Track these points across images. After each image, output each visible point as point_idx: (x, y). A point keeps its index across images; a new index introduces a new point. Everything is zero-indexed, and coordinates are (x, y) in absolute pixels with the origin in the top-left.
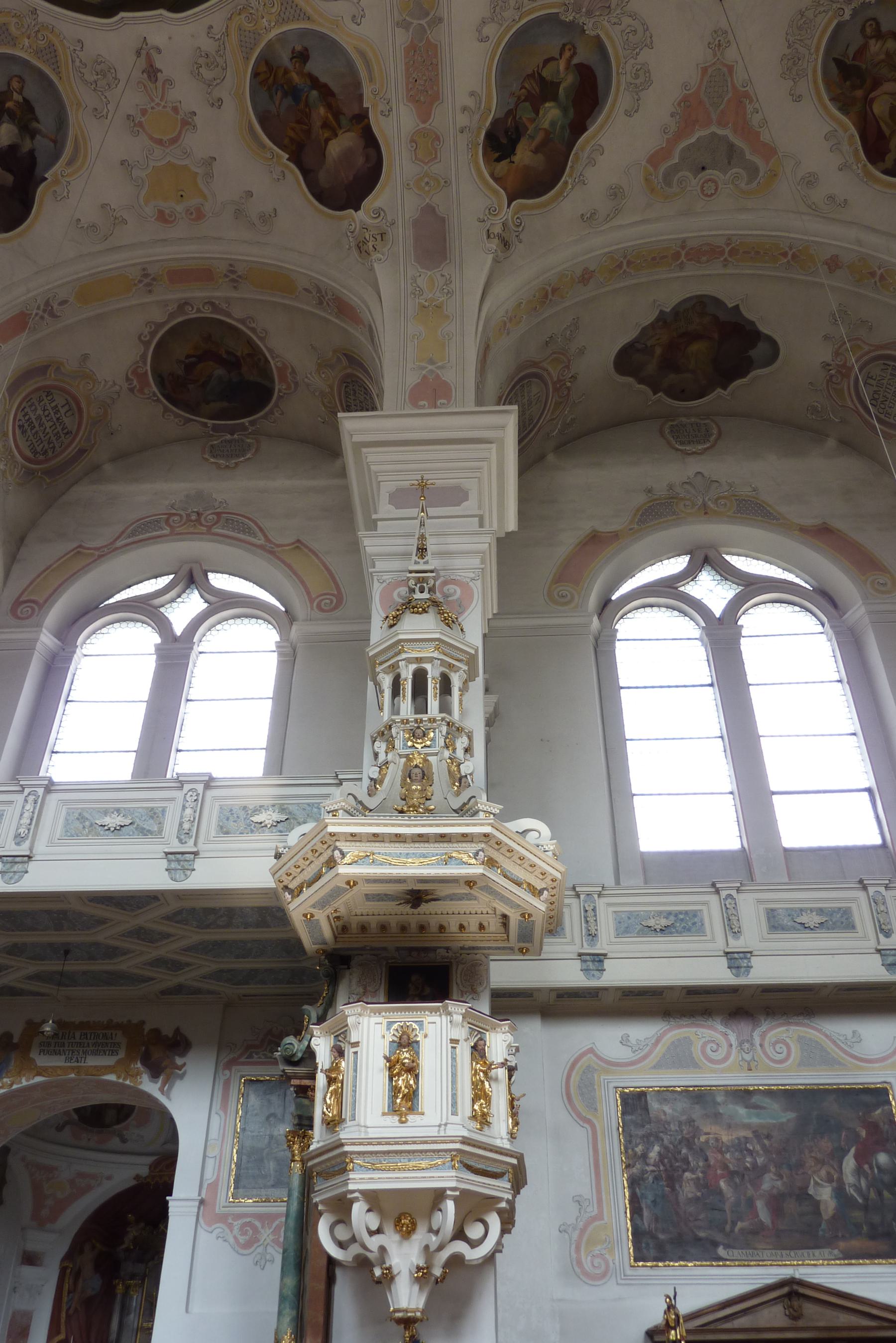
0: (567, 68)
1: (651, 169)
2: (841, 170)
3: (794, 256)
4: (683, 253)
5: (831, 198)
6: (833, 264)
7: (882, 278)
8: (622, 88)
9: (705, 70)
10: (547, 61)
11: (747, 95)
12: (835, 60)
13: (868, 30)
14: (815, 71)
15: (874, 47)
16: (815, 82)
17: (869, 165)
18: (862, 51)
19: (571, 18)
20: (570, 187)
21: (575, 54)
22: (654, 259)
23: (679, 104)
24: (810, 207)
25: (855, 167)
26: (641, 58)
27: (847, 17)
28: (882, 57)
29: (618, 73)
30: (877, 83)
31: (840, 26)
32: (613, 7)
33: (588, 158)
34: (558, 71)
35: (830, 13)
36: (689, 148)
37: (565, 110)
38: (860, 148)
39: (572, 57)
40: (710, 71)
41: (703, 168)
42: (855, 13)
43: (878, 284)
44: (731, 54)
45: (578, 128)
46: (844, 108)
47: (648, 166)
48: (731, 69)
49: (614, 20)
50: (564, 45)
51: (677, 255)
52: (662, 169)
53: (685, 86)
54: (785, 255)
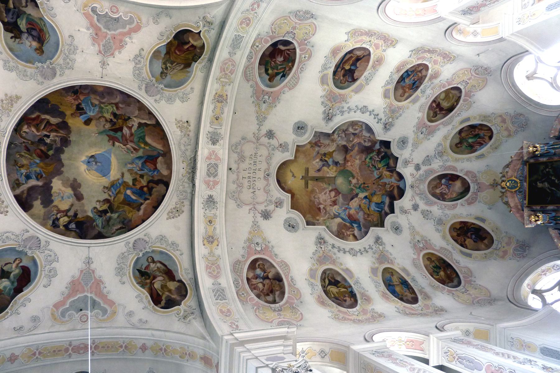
0: (17, 266)
1: (55, 309)
2: (143, 309)
3: (126, 347)
4: (70, 348)
5: (140, 320)
6: (144, 348)
7: (165, 350)
8: (43, 276)
9: (82, 271)
10: (6, 264)
11: (101, 281)
12: (137, 269)
13: (150, 260)
14: (129, 273)
15: (152, 265)
16: (130, 277)
17: (155, 306)
18: (147, 267)
19: (21, 249)
20: (10, 314)
21: (21, 262)
22: (54, 351)
23: (70, 284)
24: (131, 325)
25: (149, 307)
26: (53, 266)
27: (141, 255)
28: (156, 269)
29: (41, 271)
30: (155, 278)
31: (138, 259)
32: (41, 247)
33: (22, 303)
34: (12, 268)
35: (134, 254)
36: (74, 301)
37: (12, 283)
38: (151, 300)
39: (19, 263)
40: (84, 272)
41: (81, 310)
42: (144, 255)
43: (164, 354)
44: (93, 266)
45: (18, 290)
46: (143, 286)
47: (54, 308)
48: (93, 271)
49: (41, 251)
50: (16, 259)
51: (67, 350)
52: (61, 310)
53: (73, 277)
54: (121, 347)
